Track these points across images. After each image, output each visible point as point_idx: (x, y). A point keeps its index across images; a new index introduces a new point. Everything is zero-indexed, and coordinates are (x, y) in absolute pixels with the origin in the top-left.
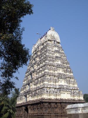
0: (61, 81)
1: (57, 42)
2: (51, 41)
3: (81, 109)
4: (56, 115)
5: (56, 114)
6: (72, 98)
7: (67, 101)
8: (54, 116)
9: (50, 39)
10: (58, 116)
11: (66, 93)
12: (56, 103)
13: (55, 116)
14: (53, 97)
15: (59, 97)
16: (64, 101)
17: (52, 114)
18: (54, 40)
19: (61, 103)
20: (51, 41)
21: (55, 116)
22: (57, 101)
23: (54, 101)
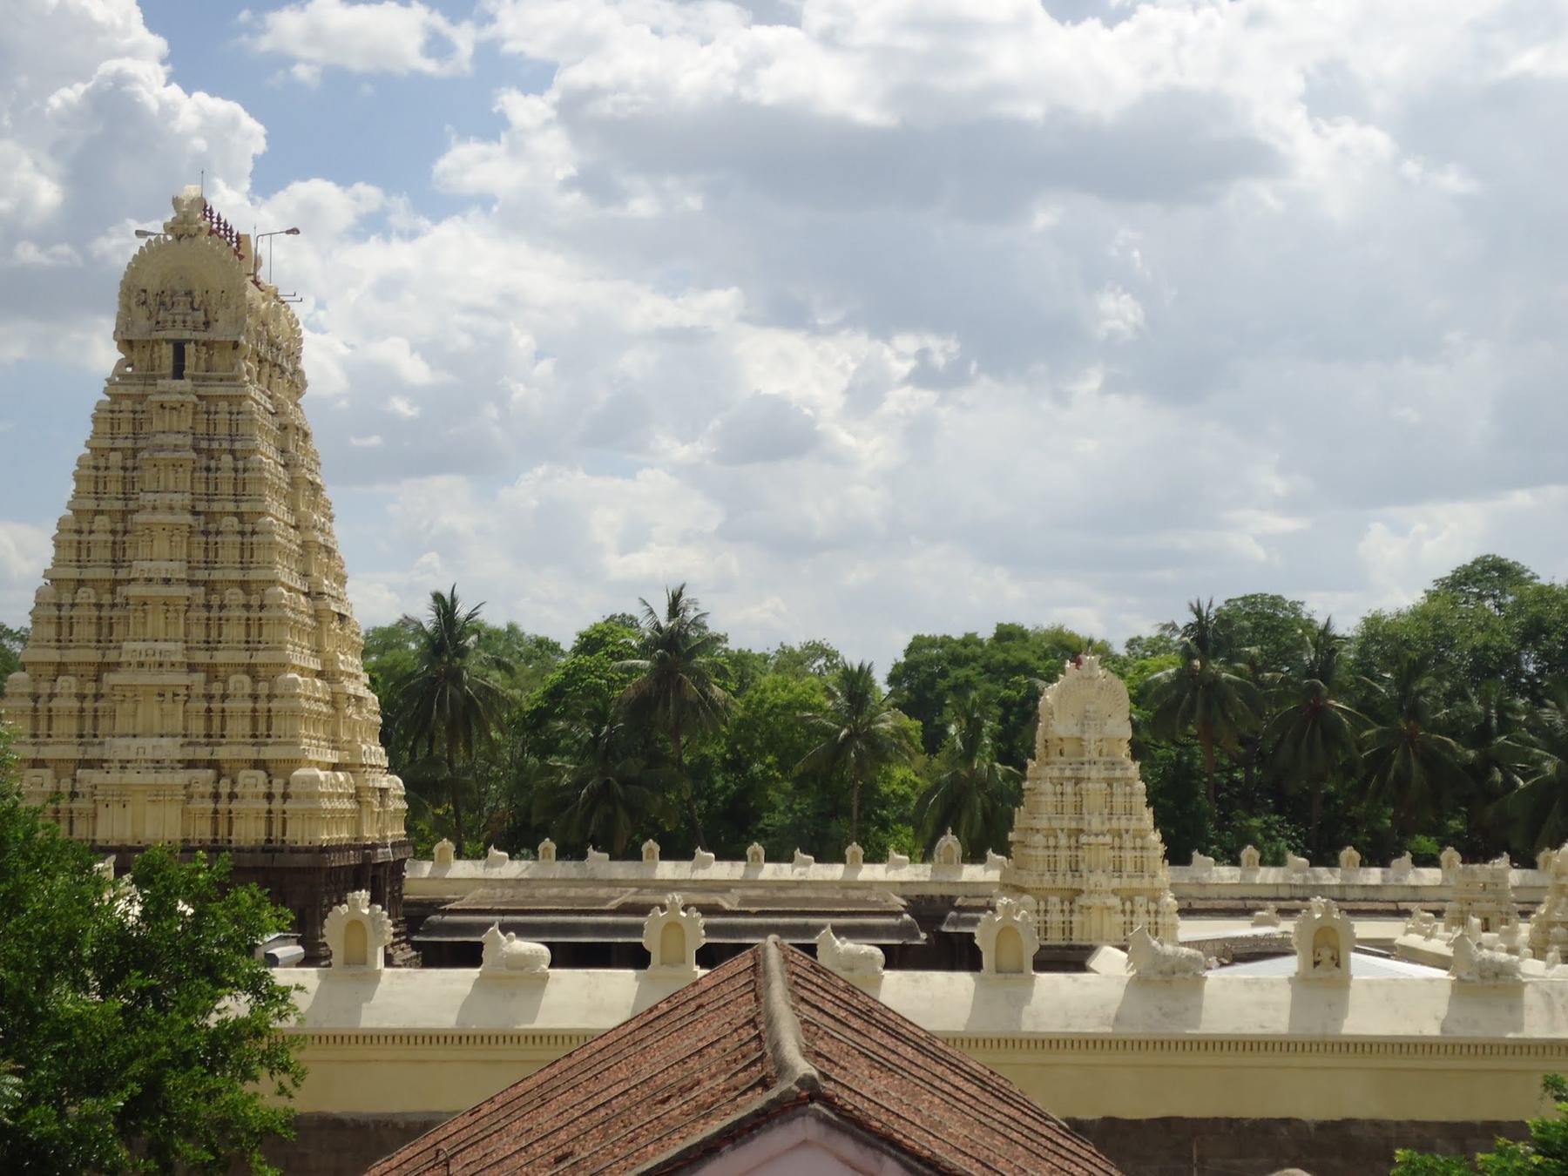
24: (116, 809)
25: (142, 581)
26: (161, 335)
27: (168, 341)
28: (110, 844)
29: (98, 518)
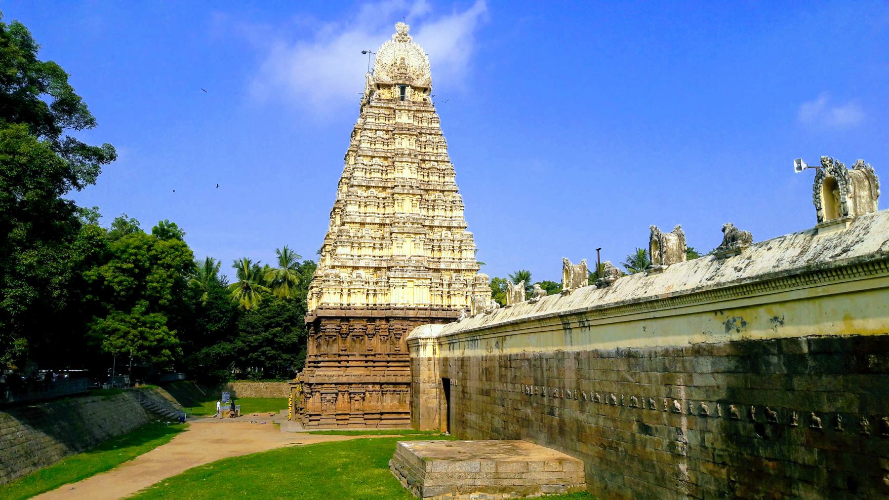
0: (399, 241)
1: (415, 88)
2: (388, 86)
3: (430, 342)
4: (366, 361)
5: (370, 358)
6: (437, 301)
7: (411, 314)
8: (359, 364)
9: (386, 79)
10: (376, 364)
11: (410, 284)
12: (372, 319)
13: (363, 364)
14: (358, 300)
15: (381, 300)
16: (401, 314)
17: (350, 358)
18: (400, 82)
19: (387, 319)
20: (388, 86)
21: (363, 364)
22: (376, 314)
23: (360, 313)
24: (399, 289)
25: (400, 187)
26: (395, 82)
27: (398, 84)
28: (397, 306)
29: (374, 159)
